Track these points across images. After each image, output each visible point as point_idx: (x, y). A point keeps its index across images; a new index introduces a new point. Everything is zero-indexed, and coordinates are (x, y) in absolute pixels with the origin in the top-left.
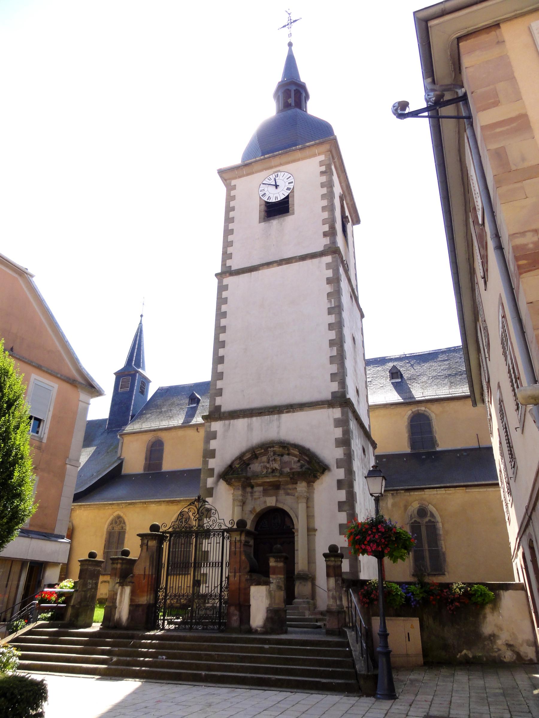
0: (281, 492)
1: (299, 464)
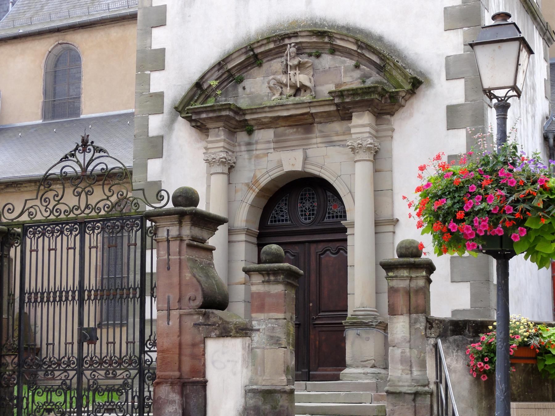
1: (357, 74)
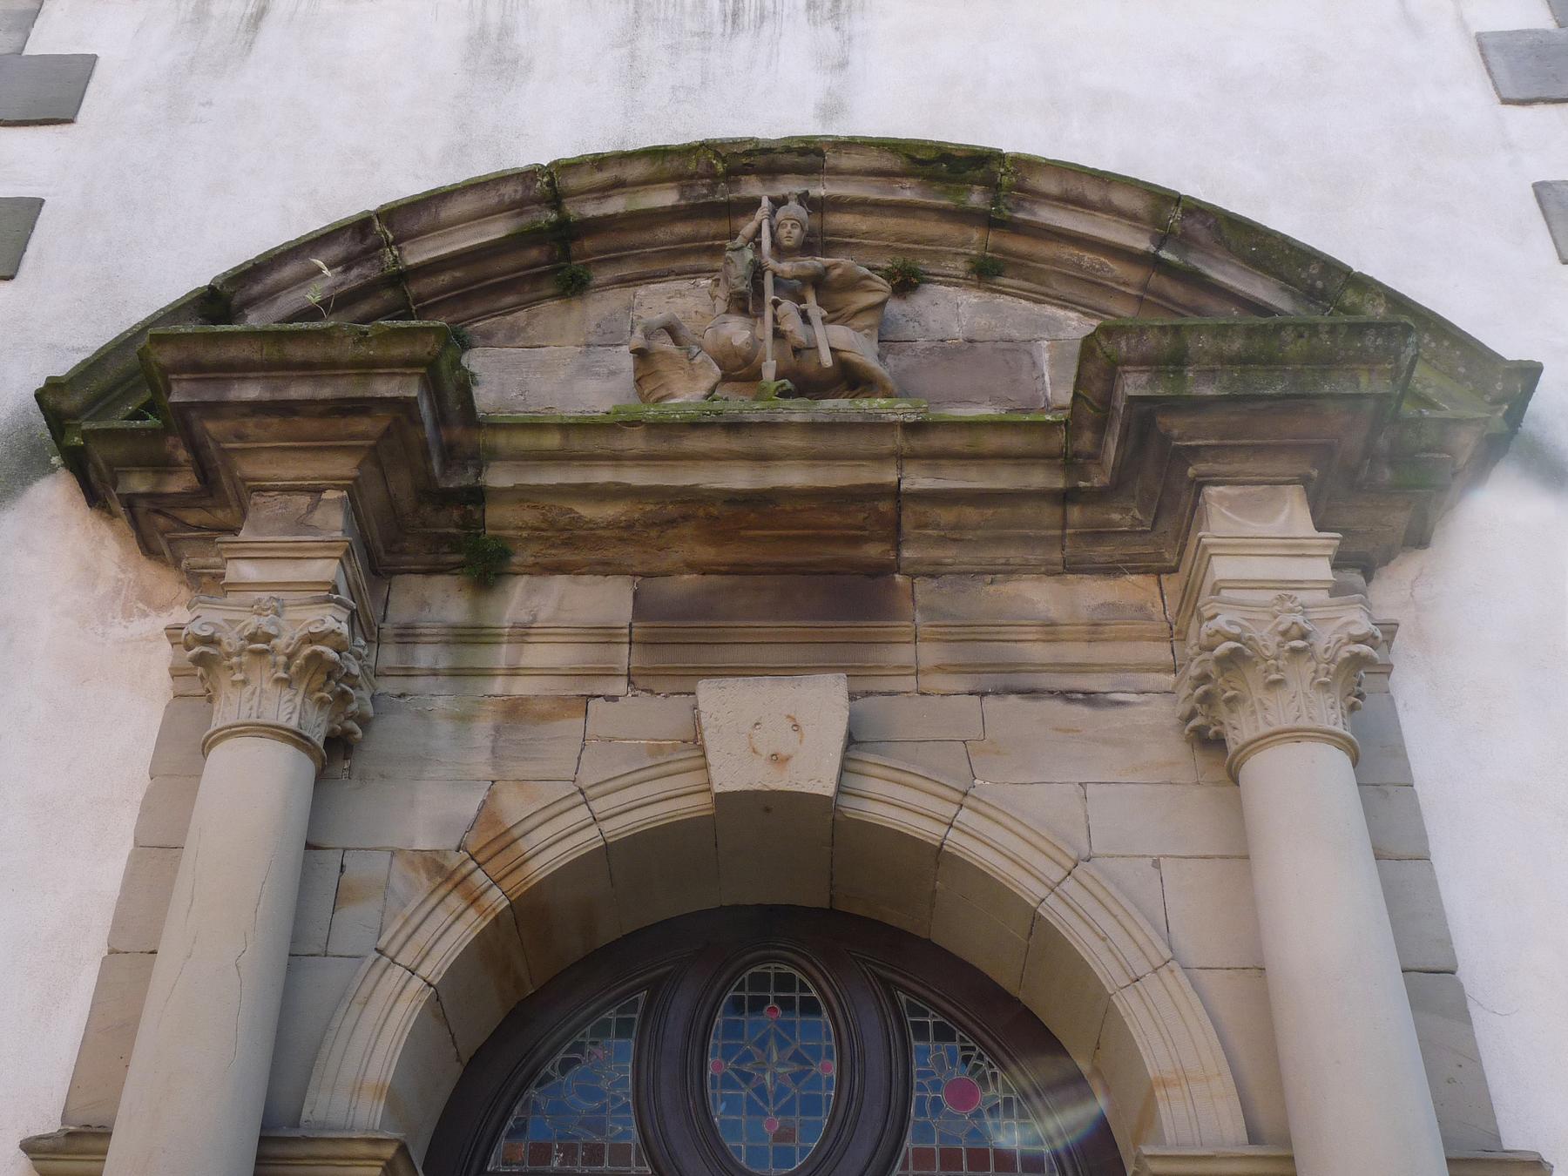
0: (913, 650)
